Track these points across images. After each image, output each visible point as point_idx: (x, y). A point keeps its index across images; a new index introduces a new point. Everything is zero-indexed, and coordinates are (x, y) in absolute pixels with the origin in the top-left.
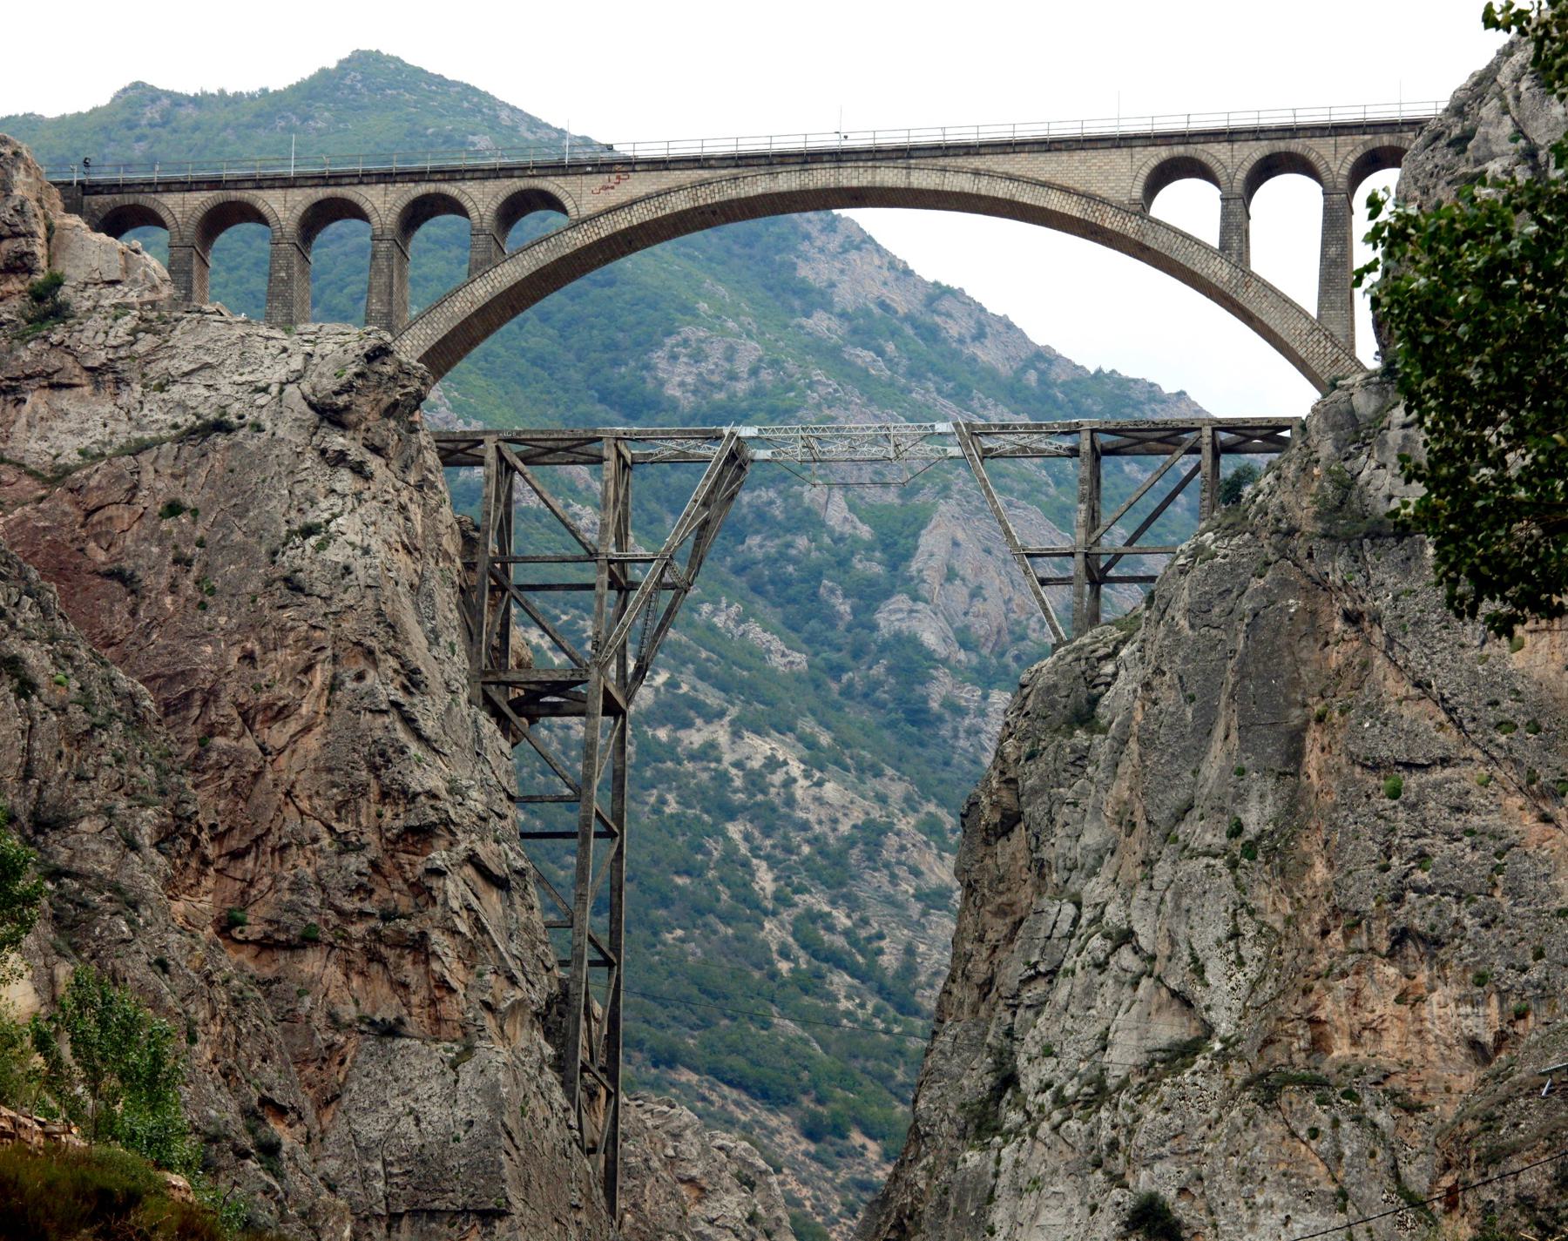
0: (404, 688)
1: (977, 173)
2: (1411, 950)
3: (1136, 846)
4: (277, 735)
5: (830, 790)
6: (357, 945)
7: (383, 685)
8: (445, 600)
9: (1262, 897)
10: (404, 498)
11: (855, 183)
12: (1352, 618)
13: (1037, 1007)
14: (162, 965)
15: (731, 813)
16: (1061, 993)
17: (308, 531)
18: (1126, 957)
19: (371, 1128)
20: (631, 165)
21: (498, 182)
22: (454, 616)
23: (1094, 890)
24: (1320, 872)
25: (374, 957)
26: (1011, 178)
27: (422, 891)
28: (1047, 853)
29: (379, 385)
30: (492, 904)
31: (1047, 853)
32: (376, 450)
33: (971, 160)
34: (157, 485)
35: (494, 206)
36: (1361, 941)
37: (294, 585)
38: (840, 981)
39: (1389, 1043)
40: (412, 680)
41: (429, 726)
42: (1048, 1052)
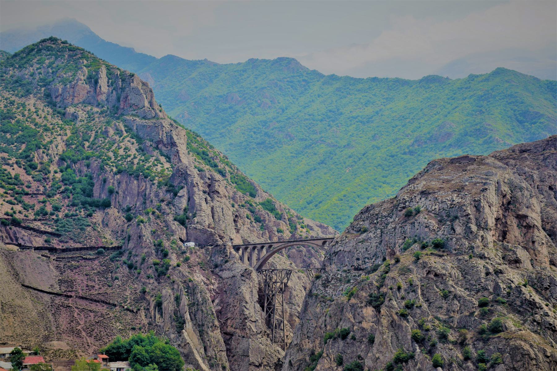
4: (236, 308)
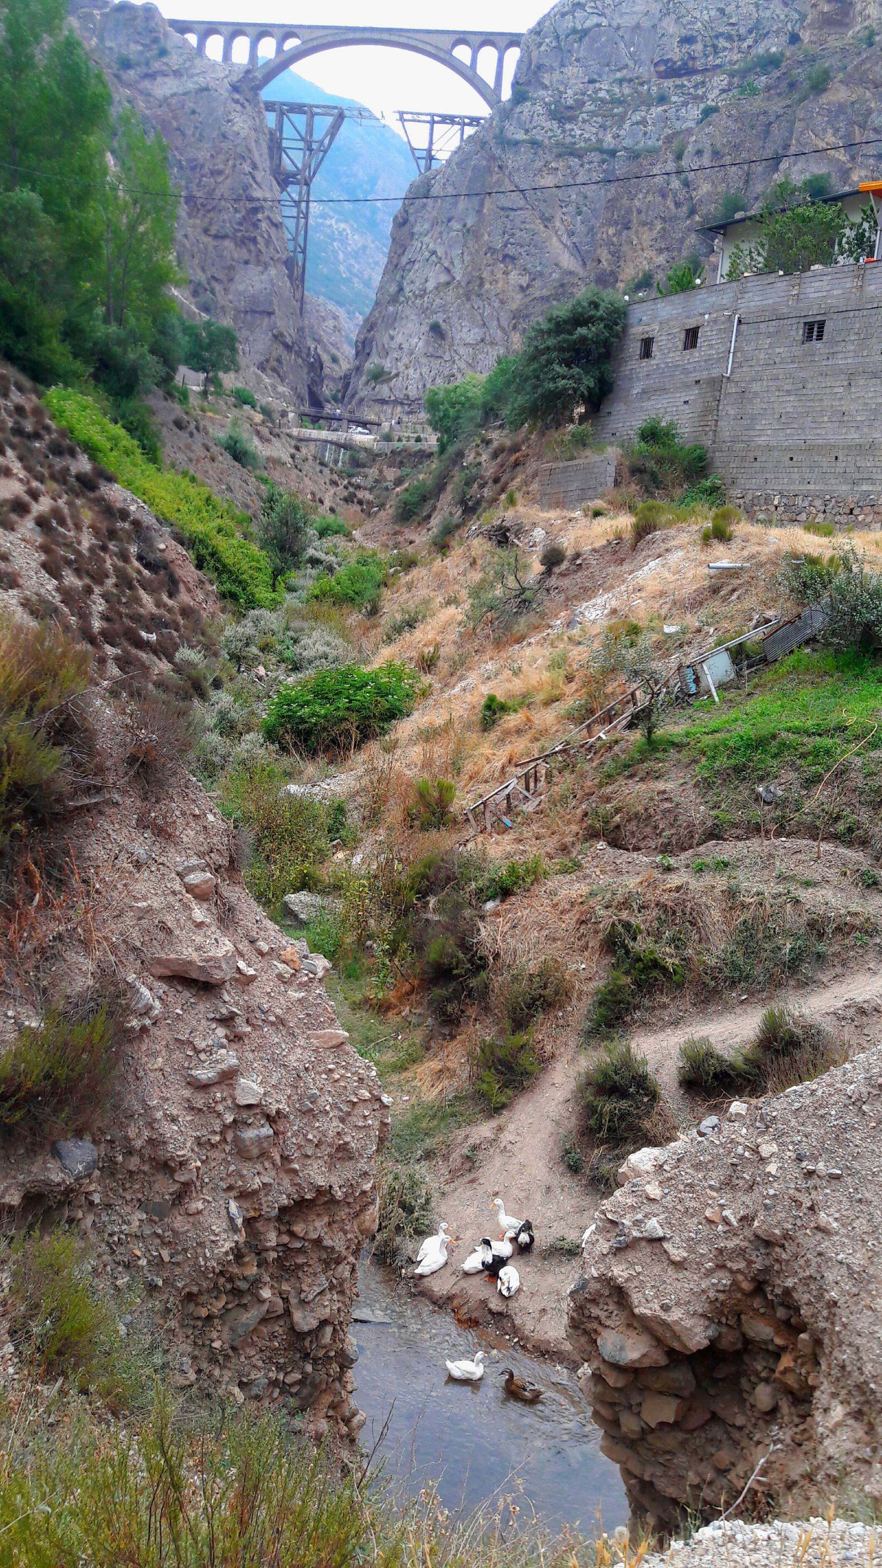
2: (507, 260)
3: (439, 229)
4: (220, 179)
5: (356, 237)
7: (247, 168)
8: (264, 146)
9: (470, 243)
12: (500, 167)
13: (410, 271)
14: (186, 236)
15: (334, 240)
16: (416, 266)
17: (229, 121)
18: (434, 258)
19: (241, 288)
22: (266, 151)
23: (426, 239)
24: (486, 237)
25: (243, 242)
27: (256, 226)
28: (415, 230)
30: (273, 231)
31: (415, 230)
34: (190, 105)
36: (495, 257)
37: (224, 136)
38: (355, 280)
39: (500, 285)
40: (255, 166)
41: (259, 179)
42: (412, 282)
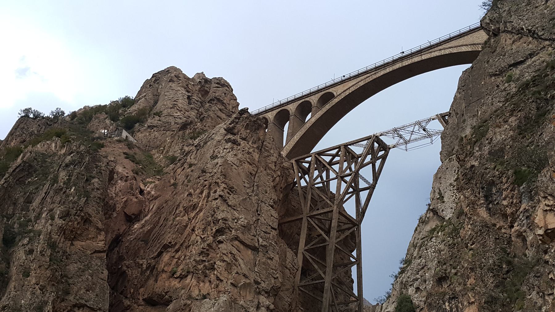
0: (229, 193)
1: (440, 50)
6: (200, 272)
10: (251, 150)
11: (407, 64)
20: (350, 79)
21: (318, 94)
26: (450, 48)
29: (243, 121)
32: (244, 139)
33: (439, 47)
35: (317, 99)
